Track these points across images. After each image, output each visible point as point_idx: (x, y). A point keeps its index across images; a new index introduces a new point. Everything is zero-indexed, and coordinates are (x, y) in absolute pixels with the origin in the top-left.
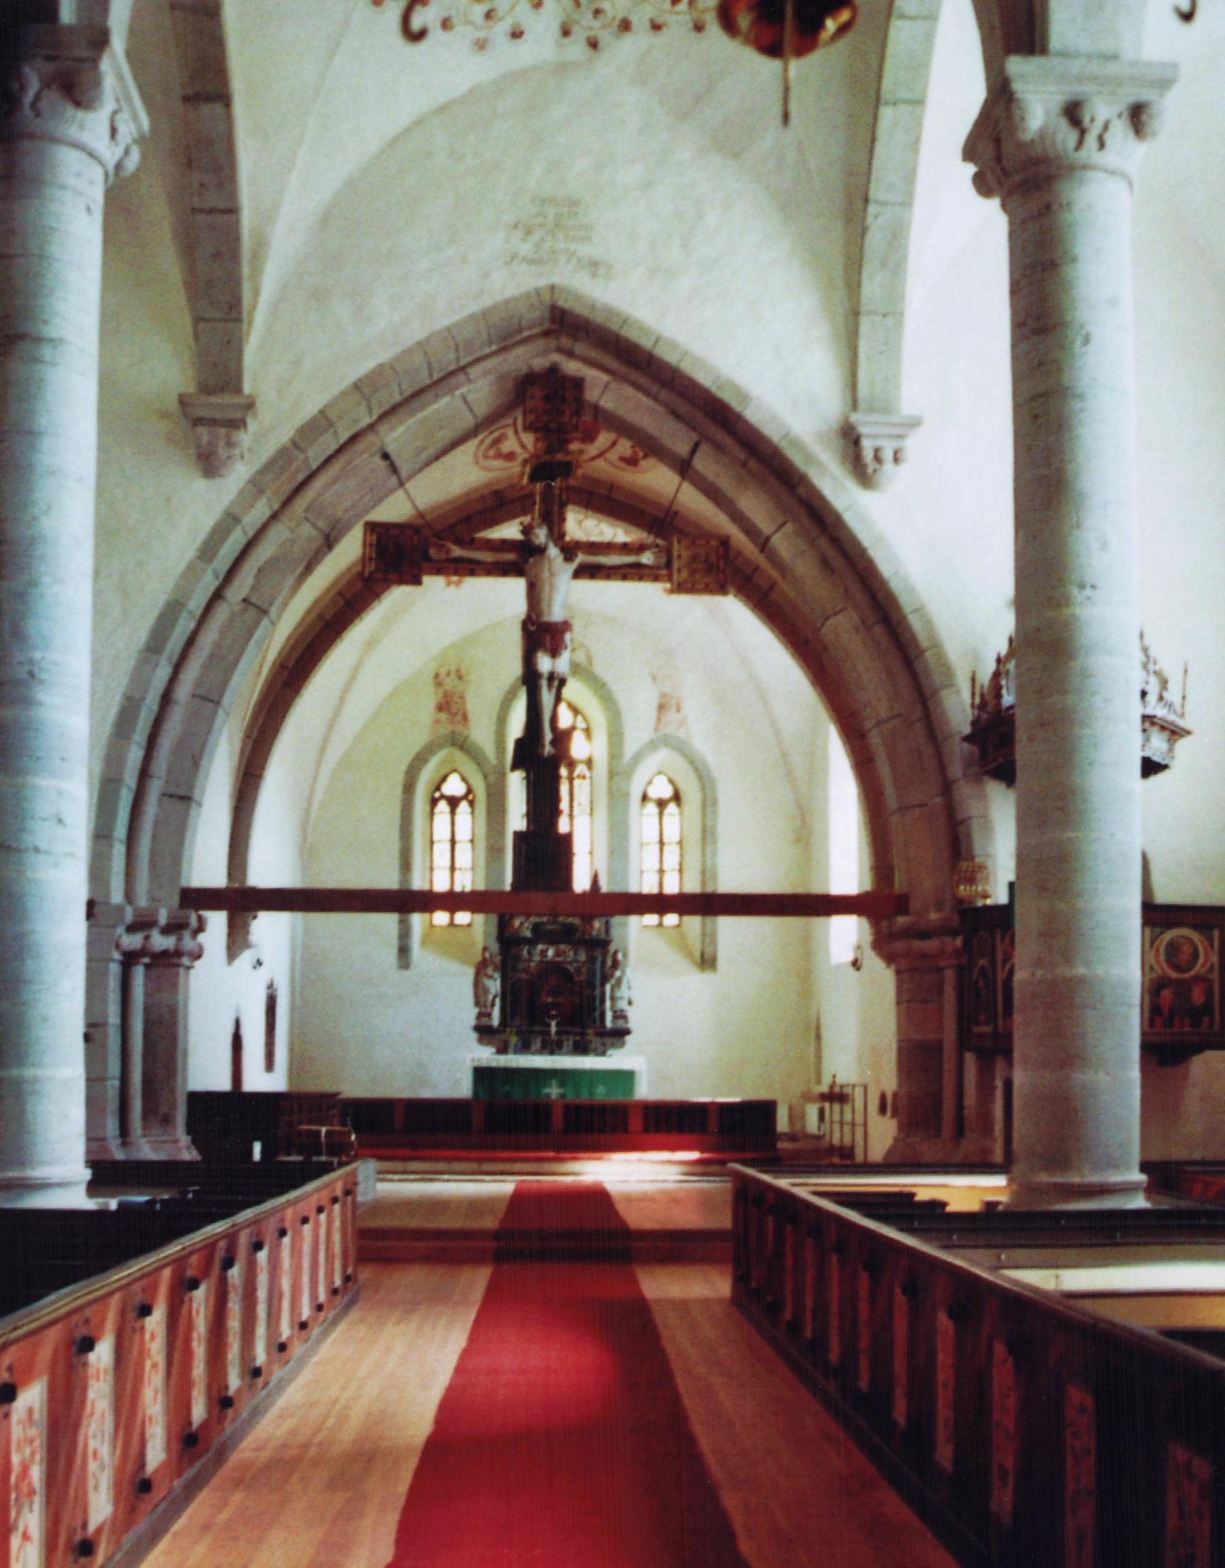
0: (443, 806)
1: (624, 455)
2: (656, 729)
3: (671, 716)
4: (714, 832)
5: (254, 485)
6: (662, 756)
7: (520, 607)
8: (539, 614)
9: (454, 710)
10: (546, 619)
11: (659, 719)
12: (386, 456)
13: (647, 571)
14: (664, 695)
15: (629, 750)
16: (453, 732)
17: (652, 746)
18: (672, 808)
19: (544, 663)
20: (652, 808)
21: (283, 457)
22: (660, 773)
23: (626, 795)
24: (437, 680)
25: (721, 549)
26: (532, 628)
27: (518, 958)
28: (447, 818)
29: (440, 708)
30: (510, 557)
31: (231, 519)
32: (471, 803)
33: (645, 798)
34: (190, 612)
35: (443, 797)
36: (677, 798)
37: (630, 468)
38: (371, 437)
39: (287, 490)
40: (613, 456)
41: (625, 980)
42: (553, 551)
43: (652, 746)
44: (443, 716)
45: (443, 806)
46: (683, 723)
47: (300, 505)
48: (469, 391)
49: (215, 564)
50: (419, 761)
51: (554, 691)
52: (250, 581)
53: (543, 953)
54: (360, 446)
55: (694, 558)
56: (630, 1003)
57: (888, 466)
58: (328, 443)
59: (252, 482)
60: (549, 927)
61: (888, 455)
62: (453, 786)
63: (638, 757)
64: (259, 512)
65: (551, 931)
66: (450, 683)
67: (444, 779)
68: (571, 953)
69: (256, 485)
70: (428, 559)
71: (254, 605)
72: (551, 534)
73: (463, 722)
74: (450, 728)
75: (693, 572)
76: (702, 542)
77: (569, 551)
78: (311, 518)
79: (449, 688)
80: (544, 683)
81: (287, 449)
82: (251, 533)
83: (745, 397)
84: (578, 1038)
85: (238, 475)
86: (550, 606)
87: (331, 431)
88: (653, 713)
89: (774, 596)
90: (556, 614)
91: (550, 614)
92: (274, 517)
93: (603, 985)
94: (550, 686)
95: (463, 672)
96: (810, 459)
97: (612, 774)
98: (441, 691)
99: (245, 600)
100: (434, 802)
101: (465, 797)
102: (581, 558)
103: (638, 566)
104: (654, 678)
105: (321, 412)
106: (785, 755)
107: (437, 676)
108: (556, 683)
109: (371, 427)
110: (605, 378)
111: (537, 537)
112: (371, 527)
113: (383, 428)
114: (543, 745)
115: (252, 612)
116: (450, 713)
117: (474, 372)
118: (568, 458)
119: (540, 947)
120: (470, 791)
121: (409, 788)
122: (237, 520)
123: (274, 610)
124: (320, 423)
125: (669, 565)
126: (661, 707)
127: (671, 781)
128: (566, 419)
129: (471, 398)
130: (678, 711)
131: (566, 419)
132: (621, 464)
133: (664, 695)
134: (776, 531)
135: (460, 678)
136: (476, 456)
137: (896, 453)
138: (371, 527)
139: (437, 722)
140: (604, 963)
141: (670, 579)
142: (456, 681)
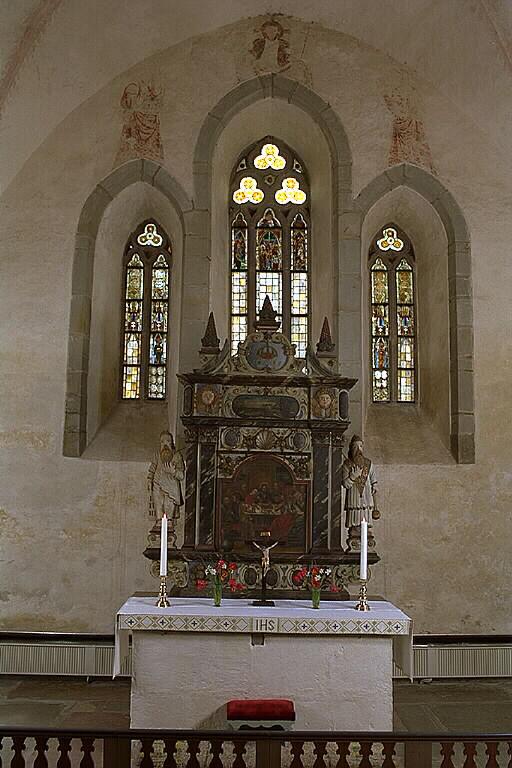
4: (467, 285)
11: (395, 150)
14: (400, 121)
15: (359, 185)
17: (389, 181)
27: (209, 449)
28: (139, 274)
33: (374, 251)
36: (409, 252)
41: (368, 483)
44: (132, 140)
50: (102, 196)
53: (250, 441)
56: (375, 515)
60: (259, 403)
62: (151, 238)
65: (264, 410)
66: (139, 106)
68: (291, 444)
84: (299, 567)
88: (388, 142)
93: (336, 488)
95: (157, 92)
97: (336, 211)
107: (125, 95)
119: (244, 431)
120: (167, 244)
121: (88, 229)
126: (397, 135)
133: (400, 121)
140: (337, 457)
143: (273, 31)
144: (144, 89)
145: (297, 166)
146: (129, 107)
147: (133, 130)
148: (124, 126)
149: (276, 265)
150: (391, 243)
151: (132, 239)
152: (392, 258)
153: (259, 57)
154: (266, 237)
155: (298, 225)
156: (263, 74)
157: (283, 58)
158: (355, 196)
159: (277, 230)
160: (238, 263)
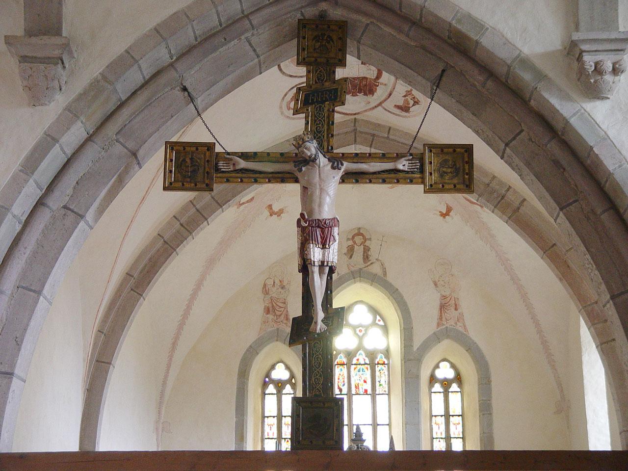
0: (271, 389)
1: (397, 104)
2: (438, 325)
3: (451, 313)
5: (69, 111)
6: (445, 346)
7: (295, 209)
8: (311, 213)
9: (278, 313)
10: (317, 216)
11: (441, 318)
12: (185, 89)
13: (401, 175)
14: (444, 297)
16: (278, 329)
17: (436, 338)
18: (454, 387)
19: (316, 254)
20: (437, 387)
21: (95, 89)
22: (444, 360)
23: (418, 377)
24: (265, 291)
25: (466, 155)
26: (304, 224)
29: (267, 311)
30: (288, 167)
31: (49, 140)
32: (294, 386)
33: (433, 379)
34: (14, 216)
35: (272, 381)
36: (458, 379)
37: (404, 114)
38: (172, 74)
39: (99, 116)
40: (389, 104)
42: (322, 160)
43: (436, 338)
44: (270, 317)
45: (271, 389)
46: (460, 318)
47: (111, 129)
48: (253, 35)
49: (36, 175)
51: (325, 277)
52: (70, 191)
54: (163, 80)
55: (444, 163)
57: (608, 78)
58: (134, 77)
59: (68, 109)
61: (608, 66)
63: (426, 346)
64: (76, 133)
66: (274, 292)
67: (273, 367)
69: (72, 112)
70: (217, 170)
71: (73, 211)
72: (320, 146)
73: (285, 321)
74: (276, 327)
75: (441, 176)
76: (451, 150)
77: (336, 161)
78: (121, 140)
79: (274, 295)
80: (316, 270)
81: (98, 82)
82: (69, 152)
83: (481, 27)
85: (59, 102)
86: (320, 205)
87: (136, 66)
88: (436, 312)
89: (523, 209)
90: (326, 212)
91: (320, 212)
92: (90, 139)
94: (321, 272)
96: (541, 76)
98: (268, 297)
99: (65, 207)
100: (265, 385)
101: (289, 381)
102: (346, 166)
103: (396, 171)
104: (436, 285)
105: (127, 52)
106: (544, 343)
107: (265, 285)
108: (327, 269)
109: (171, 65)
110: (365, 20)
111: (309, 149)
112: (171, 146)
113: (179, 66)
114: (316, 323)
115: (71, 216)
116: (275, 315)
117: (256, 19)
118: (335, 86)
120: (292, 376)
122: (55, 140)
123: (90, 216)
124: (127, 60)
125: (422, 170)
126: (443, 307)
127: (453, 366)
128: (332, 55)
129: (254, 40)
130: (456, 309)
131: (332, 55)
132: (398, 111)
134: (514, 138)
135: (283, 287)
136: (281, 107)
137: (614, 64)
138: (171, 146)
139: (265, 322)
141: (423, 182)
142: (280, 290)
143: (358, 239)
144: (277, 282)
145: (379, 321)
146: (267, 294)
147: (271, 309)
148: (265, 306)
149: (366, 391)
150: (445, 372)
151: (268, 375)
152: (446, 384)
153: (351, 257)
154: (359, 371)
155: (380, 362)
156: (353, 269)
157: (366, 258)
158: (415, 349)
159: (366, 366)
160: (341, 390)
